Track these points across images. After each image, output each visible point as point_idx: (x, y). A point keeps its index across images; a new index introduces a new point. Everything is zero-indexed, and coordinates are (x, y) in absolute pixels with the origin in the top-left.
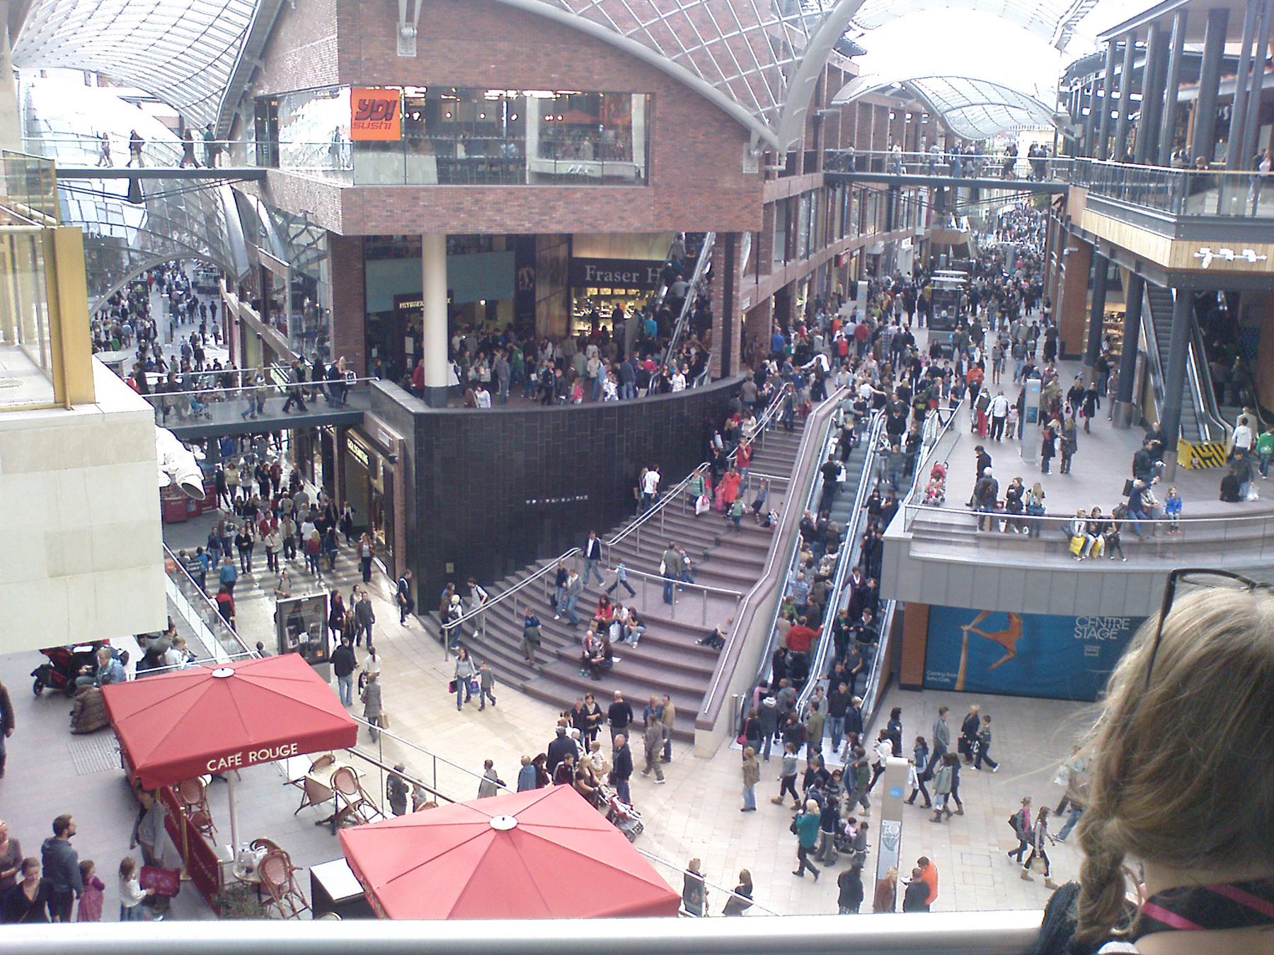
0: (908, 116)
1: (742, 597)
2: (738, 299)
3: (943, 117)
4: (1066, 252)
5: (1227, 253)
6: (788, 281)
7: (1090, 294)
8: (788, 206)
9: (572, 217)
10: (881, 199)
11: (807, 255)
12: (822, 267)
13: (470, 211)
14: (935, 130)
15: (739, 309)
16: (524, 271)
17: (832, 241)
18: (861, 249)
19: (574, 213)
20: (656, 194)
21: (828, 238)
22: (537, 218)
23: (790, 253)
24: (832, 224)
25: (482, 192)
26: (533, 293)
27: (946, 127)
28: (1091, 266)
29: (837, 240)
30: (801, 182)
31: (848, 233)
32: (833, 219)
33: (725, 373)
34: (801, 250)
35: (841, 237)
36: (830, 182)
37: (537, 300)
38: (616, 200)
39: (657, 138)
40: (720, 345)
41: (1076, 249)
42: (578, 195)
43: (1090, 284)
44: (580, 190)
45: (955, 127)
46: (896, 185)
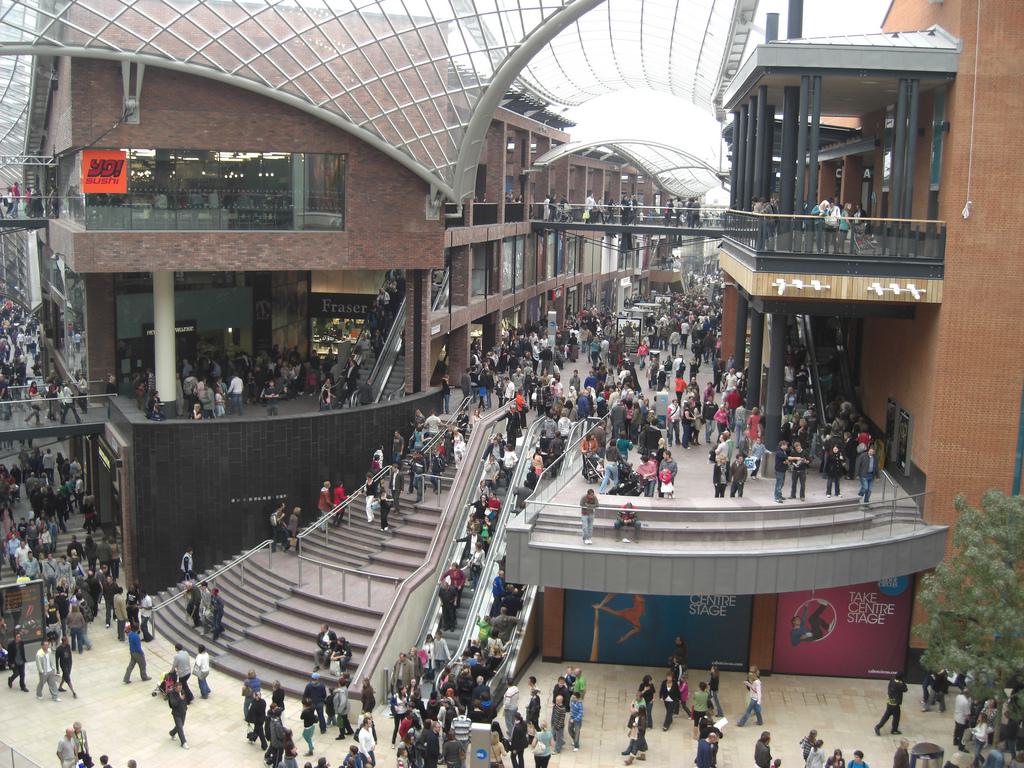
2: (425, 325)
5: (798, 283)
13: (186, 252)
16: (261, 303)
19: (278, 254)
25: (197, 236)
26: (269, 322)
37: (273, 327)
38: (315, 243)
44: (284, 234)
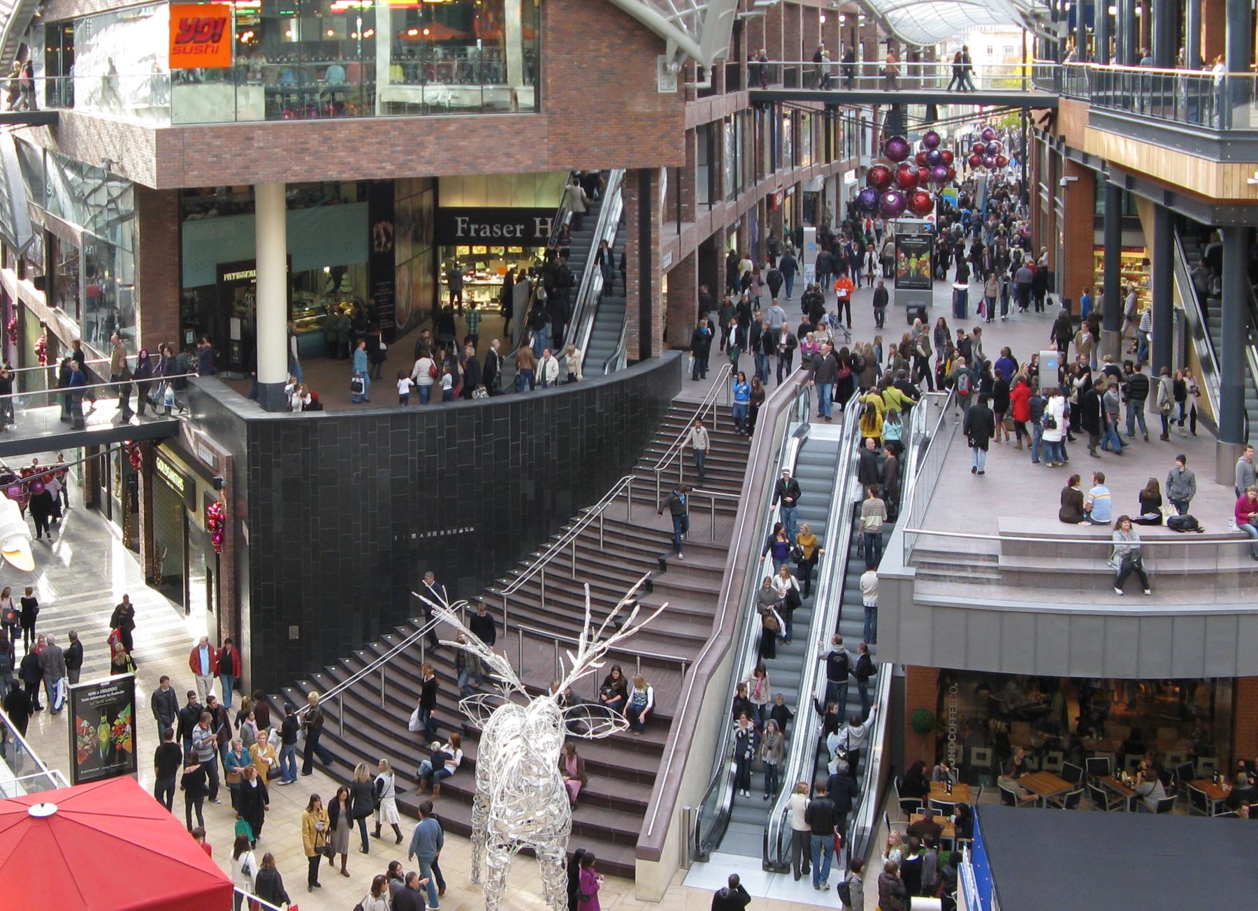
0: (842, 18)
1: (688, 665)
2: (657, 254)
3: (883, 17)
4: (1062, 182)
6: (715, 230)
7: (1100, 237)
8: (710, 132)
9: (444, 156)
10: (817, 121)
11: (735, 195)
12: (752, 210)
13: (316, 152)
14: (875, 35)
15: (659, 268)
16: (380, 227)
17: (762, 177)
18: (797, 185)
19: (447, 150)
20: (551, 123)
21: (758, 173)
22: (401, 158)
23: (714, 194)
24: (762, 155)
25: (332, 127)
26: (392, 253)
27: (889, 31)
28: (1095, 199)
29: (768, 176)
30: (725, 104)
31: (780, 166)
32: (762, 148)
33: (645, 353)
34: (728, 190)
35: (773, 171)
36: (758, 102)
37: (397, 263)
39: (550, 53)
40: (637, 317)
41: (1075, 179)
42: (452, 128)
43: (1098, 222)
44: (455, 120)
45: (899, 31)
46: (833, 105)
